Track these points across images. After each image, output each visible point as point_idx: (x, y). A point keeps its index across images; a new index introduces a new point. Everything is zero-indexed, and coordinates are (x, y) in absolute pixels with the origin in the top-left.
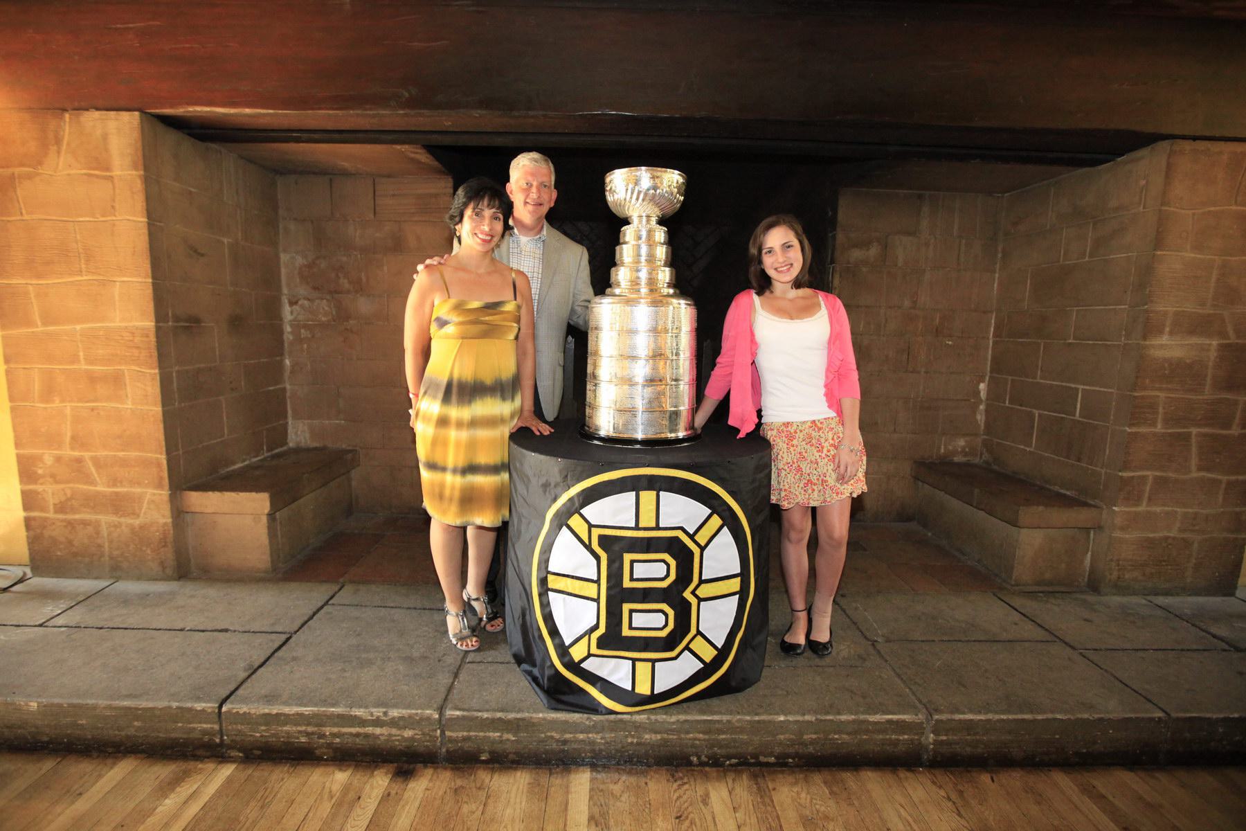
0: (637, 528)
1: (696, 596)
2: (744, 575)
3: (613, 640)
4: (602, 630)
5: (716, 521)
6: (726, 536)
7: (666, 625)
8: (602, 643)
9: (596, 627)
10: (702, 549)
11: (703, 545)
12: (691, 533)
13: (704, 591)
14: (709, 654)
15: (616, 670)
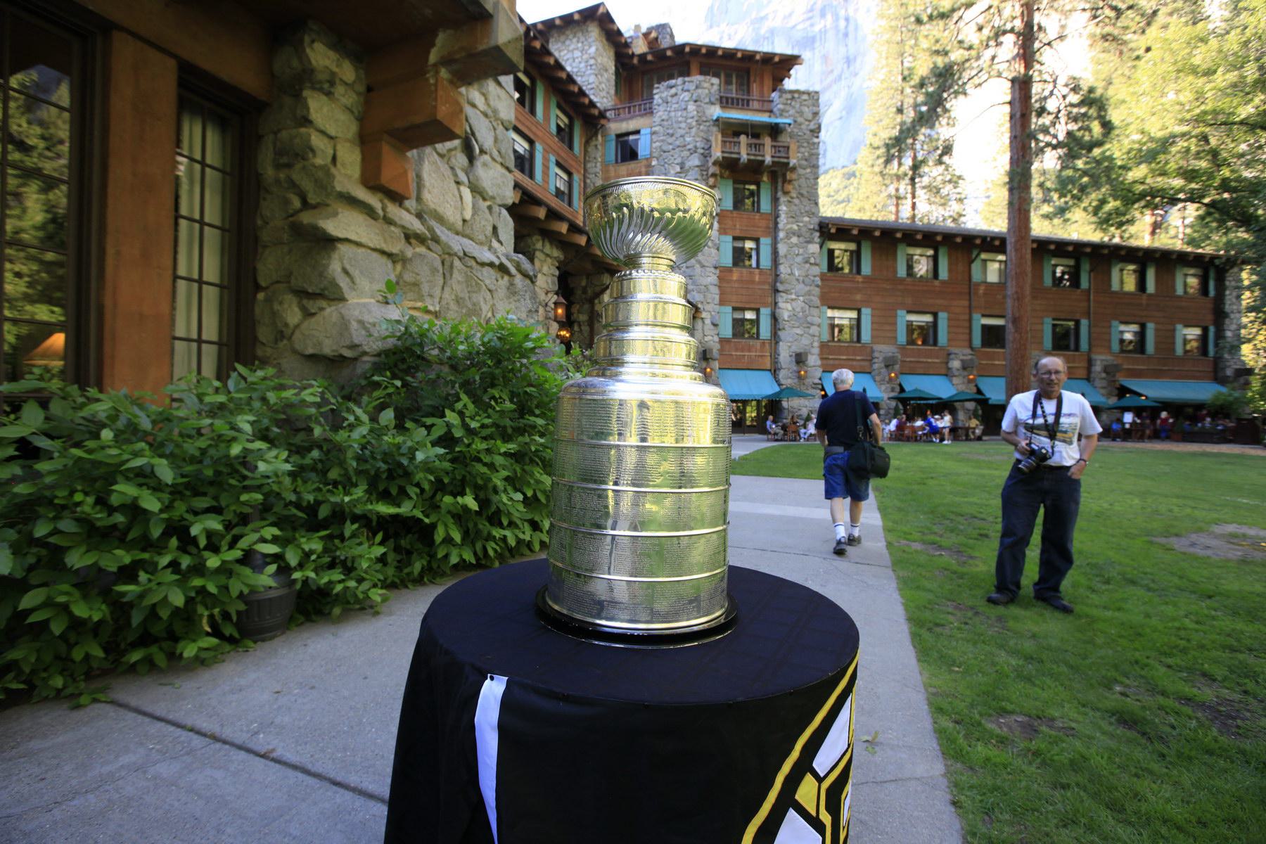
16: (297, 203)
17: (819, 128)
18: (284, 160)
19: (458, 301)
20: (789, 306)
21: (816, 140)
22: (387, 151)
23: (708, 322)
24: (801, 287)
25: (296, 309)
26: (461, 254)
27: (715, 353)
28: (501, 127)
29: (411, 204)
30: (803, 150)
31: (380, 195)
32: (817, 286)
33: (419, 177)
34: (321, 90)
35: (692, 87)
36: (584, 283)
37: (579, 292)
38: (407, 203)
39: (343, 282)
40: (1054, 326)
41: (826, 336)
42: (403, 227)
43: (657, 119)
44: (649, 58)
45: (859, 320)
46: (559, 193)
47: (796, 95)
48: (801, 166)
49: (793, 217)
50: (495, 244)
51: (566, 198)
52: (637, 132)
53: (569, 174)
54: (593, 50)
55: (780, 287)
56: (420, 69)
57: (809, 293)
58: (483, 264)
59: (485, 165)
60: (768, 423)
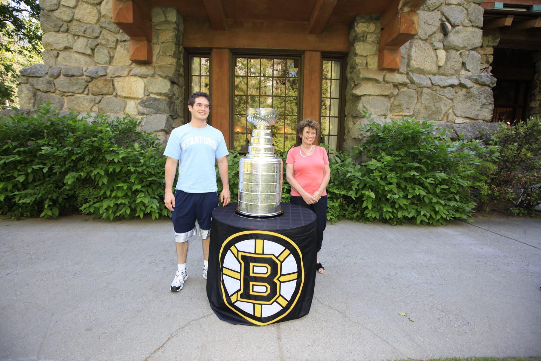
0: (255, 253)
1: (279, 281)
2: (299, 272)
3: (246, 295)
4: (242, 291)
5: (287, 252)
6: (291, 257)
7: (267, 291)
8: (242, 296)
9: (240, 290)
10: (282, 262)
11: (282, 260)
12: (277, 256)
13: (282, 279)
14: (284, 303)
15: (247, 306)
16: (353, 85)
18: (351, 70)
19: (426, 108)
22: (386, 53)
25: (352, 122)
26: (430, 85)
28: (473, 5)
29: (403, 69)
31: (384, 73)
33: (409, 56)
34: (360, 40)
38: (401, 70)
42: (393, 82)
50: (463, 72)
56: (397, 14)
58: (445, 87)
59: (457, 32)
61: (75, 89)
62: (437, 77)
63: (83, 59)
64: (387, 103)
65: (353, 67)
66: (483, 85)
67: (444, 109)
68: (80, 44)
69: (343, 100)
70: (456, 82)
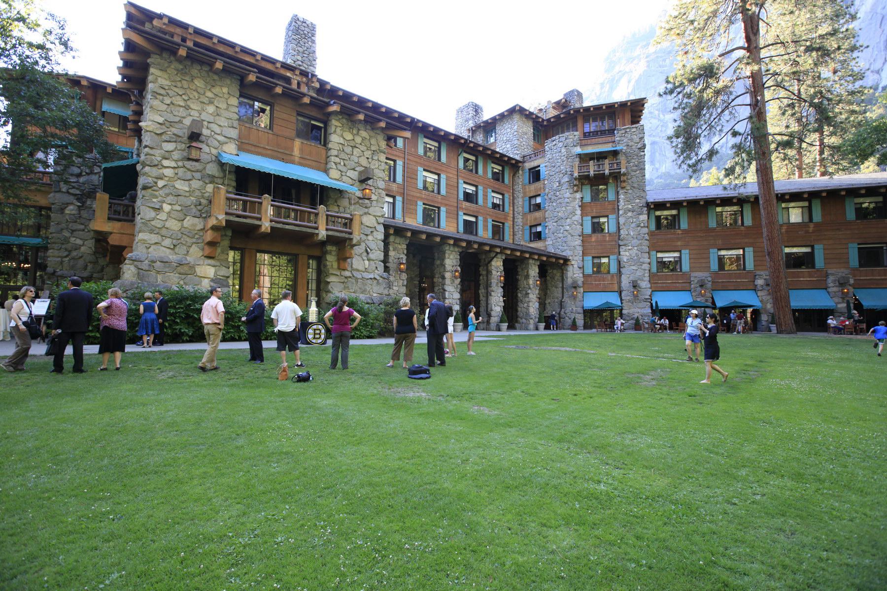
3: (314, 338)
15: (314, 341)
17: (644, 146)
19: (360, 289)
20: (627, 254)
21: (642, 153)
23: (576, 266)
24: (638, 242)
27: (580, 283)
29: (349, 269)
30: (634, 161)
32: (646, 240)
33: (352, 263)
35: (563, 139)
36: (484, 257)
37: (482, 261)
39: (331, 290)
40: (859, 248)
41: (654, 270)
43: (547, 159)
44: (552, 120)
45: (680, 257)
46: (495, 206)
47: (628, 130)
48: (632, 171)
49: (628, 201)
50: (376, 271)
51: (501, 207)
52: (539, 166)
53: (503, 195)
54: (516, 127)
55: (621, 243)
57: (641, 245)
60: (667, 321)
61: (167, 270)
62: (366, 273)
63: (168, 251)
64: (342, 286)
65: (325, 266)
66: (384, 278)
67: (368, 289)
68: (167, 242)
69: (319, 281)
70: (372, 277)
